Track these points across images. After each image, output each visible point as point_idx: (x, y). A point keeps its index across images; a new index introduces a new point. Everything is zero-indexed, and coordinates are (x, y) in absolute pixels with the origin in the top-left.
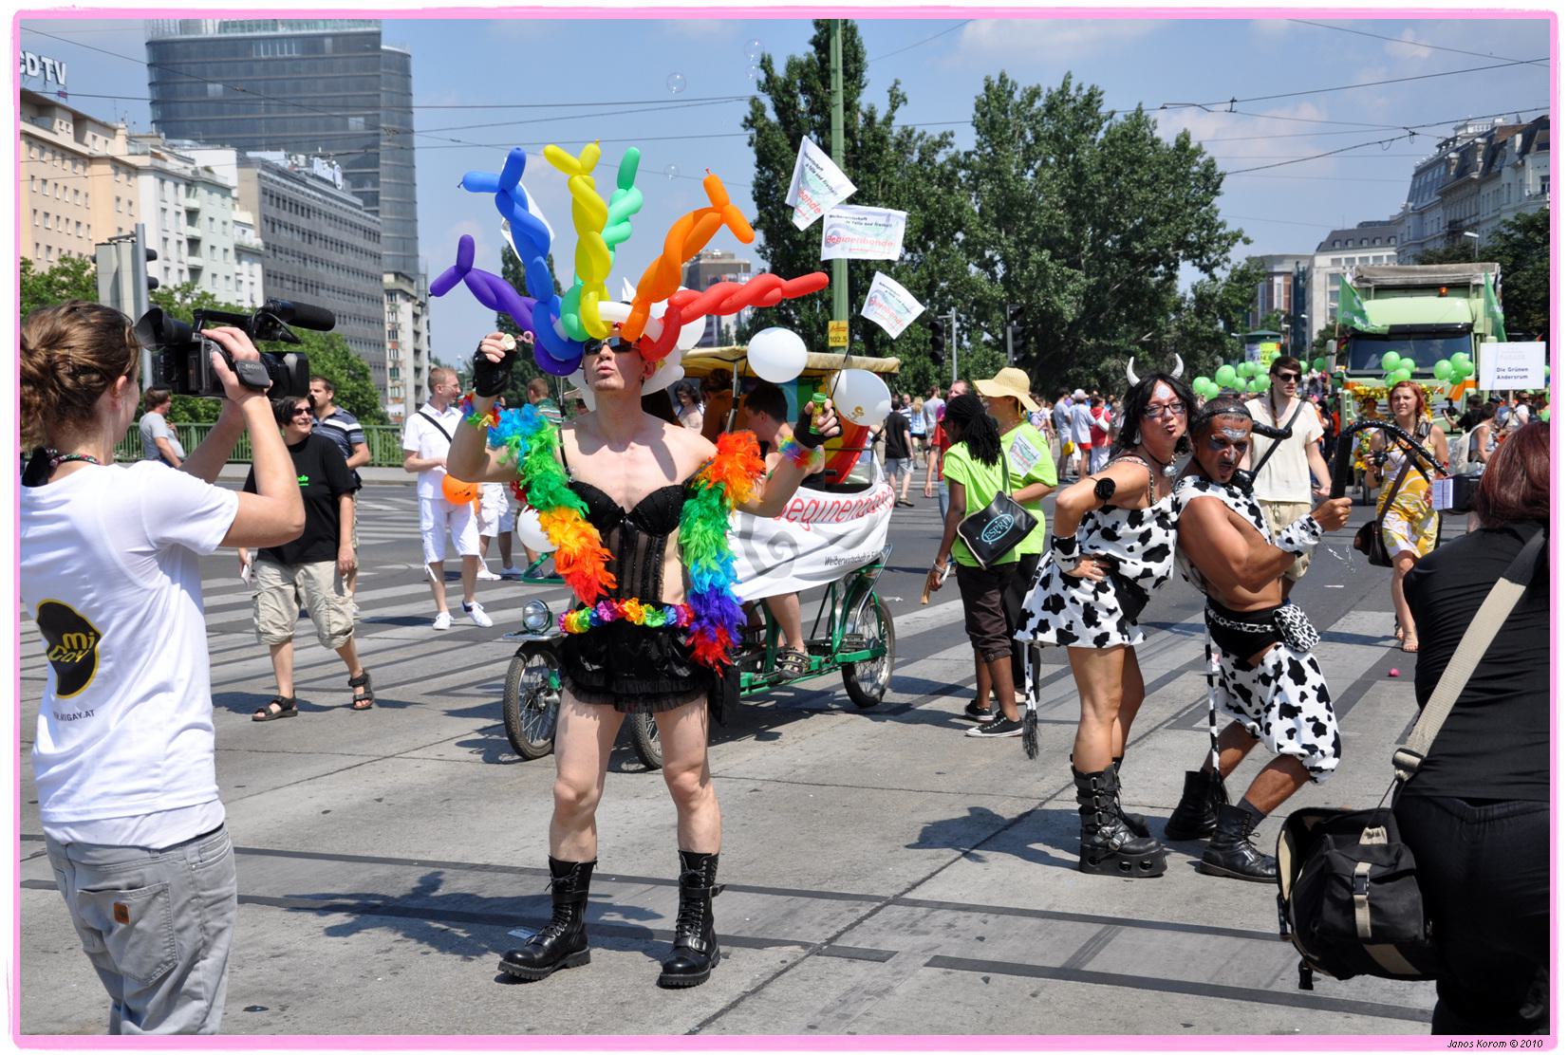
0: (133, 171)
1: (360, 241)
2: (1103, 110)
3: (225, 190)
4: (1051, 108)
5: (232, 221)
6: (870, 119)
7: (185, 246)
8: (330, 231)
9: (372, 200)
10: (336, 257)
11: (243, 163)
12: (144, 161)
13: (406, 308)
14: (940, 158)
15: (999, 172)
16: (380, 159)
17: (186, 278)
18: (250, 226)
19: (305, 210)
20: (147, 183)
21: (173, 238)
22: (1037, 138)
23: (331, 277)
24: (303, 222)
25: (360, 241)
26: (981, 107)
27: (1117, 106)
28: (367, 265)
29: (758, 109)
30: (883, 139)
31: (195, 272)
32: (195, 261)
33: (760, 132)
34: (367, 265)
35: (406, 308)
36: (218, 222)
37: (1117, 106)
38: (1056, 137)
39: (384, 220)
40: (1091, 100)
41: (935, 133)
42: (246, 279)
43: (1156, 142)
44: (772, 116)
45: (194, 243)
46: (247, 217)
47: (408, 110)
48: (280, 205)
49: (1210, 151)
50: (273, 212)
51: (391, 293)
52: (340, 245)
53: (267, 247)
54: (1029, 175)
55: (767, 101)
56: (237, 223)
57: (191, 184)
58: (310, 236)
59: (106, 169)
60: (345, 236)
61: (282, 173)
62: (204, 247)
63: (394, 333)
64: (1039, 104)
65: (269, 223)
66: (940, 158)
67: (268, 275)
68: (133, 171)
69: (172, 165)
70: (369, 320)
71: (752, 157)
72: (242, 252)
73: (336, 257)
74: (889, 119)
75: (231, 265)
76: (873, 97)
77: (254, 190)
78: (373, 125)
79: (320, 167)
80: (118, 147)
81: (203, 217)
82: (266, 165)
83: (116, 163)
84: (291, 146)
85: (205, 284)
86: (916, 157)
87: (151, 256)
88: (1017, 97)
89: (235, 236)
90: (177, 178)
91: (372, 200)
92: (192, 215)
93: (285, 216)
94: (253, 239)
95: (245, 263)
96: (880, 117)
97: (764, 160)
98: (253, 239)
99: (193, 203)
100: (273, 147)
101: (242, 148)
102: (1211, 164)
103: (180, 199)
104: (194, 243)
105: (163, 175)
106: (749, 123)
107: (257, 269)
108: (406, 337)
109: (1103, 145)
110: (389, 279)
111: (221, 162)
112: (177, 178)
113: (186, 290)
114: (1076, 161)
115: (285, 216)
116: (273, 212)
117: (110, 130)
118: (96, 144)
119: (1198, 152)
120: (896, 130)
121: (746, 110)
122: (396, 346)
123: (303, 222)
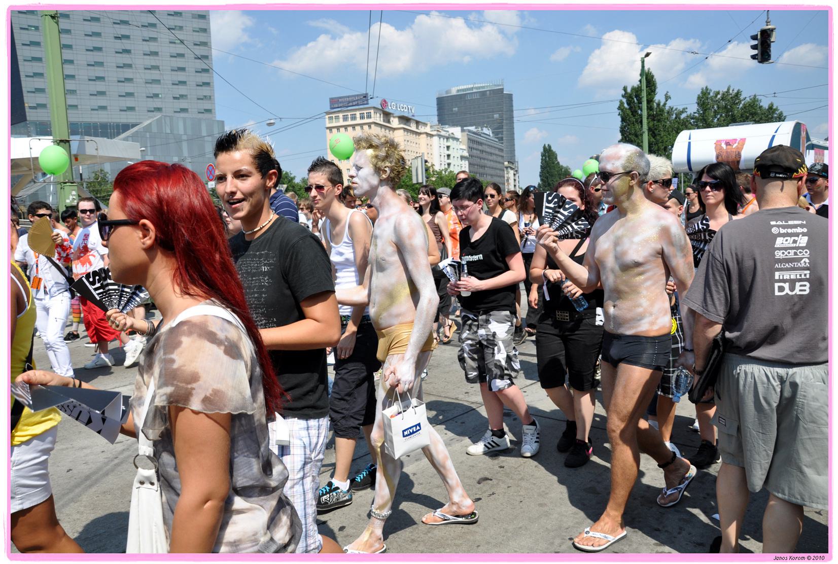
0: (432, 136)
1: (497, 152)
2: (742, 98)
3: (457, 139)
4: (723, 99)
5: (460, 148)
6: (658, 104)
8: (488, 150)
9: (501, 139)
10: (490, 157)
11: (463, 131)
12: (435, 133)
13: (512, 172)
14: (683, 116)
15: (705, 120)
16: (504, 127)
19: (481, 144)
20: (436, 139)
22: (718, 108)
23: (489, 164)
24: (480, 148)
25: (497, 152)
26: (699, 98)
27: (746, 96)
28: (499, 159)
29: (622, 103)
30: (662, 111)
31: (449, 164)
32: (449, 161)
33: (622, 110)
34: (499, 159)
35: (512, 172)
37: (746, 96)
38: (726, 107)
39: (503, 146)
40: (738, 94)
41: (680, 108)
43: (761, 107)
44: (626, 105)
45: (449, 156)
46: (464, 147)
47: (512, 111)
48: (473, 143)
49: (781, 109)
50: (471, 145)
51: (507, 168)
52: (491, 154)
54: (716, 120)
55: (624, 100)
57: (448, 138)
58: (482, 151)
59: (425, 136)
60: (493, 151)
61: (474, 133)
63: (508, 180)
64: (719, 96)
65: (470, 148)
66: (683, 116)
67: (470, 164)
68: (432, 136)
69: (443, 133)
70: (500, 176)
71: (620, 119)
72: (462, 158)
73: (490, 157)
74: (665, 104)
75: (459, 162)
76: (659, 97)
77: (465, 139)
78: (501, 116)
79: (485, 131)
80: (428, 129)
82: (469, 131)
83: (427, 134)
84: (477, 125)
85: (452, 168)
86: (674, 116)
87: (426, 161)
88: (711, 94)
89: (461, 153)
90: (444, 137)
91: (501, 139)
92: (448, 147)
93: (475, 146)
94: (466, 154)
96: (662, 104)
97: (623, 120)
98: (466, 154)
99: (448, 144)
100: (471, 125)
101: (462, 124)
102: (781, 113)
103: (445, 143)
104: (449, 156)
105: (440, 136)
106: (619, 108)
108: (511, 181)
109: (742, 109)
110: (506, 163)
111: (456, 131)
112: (444, 137)
113: (446, 170)
114: (732, 115)
115: (475, 146)
116: (471, 145)
117: (425, 124)
118: (422, 129)
119: (776, 109)
120: (667, 108)
121: (618, 104)
122: (508, 184)
123: (480, 148)
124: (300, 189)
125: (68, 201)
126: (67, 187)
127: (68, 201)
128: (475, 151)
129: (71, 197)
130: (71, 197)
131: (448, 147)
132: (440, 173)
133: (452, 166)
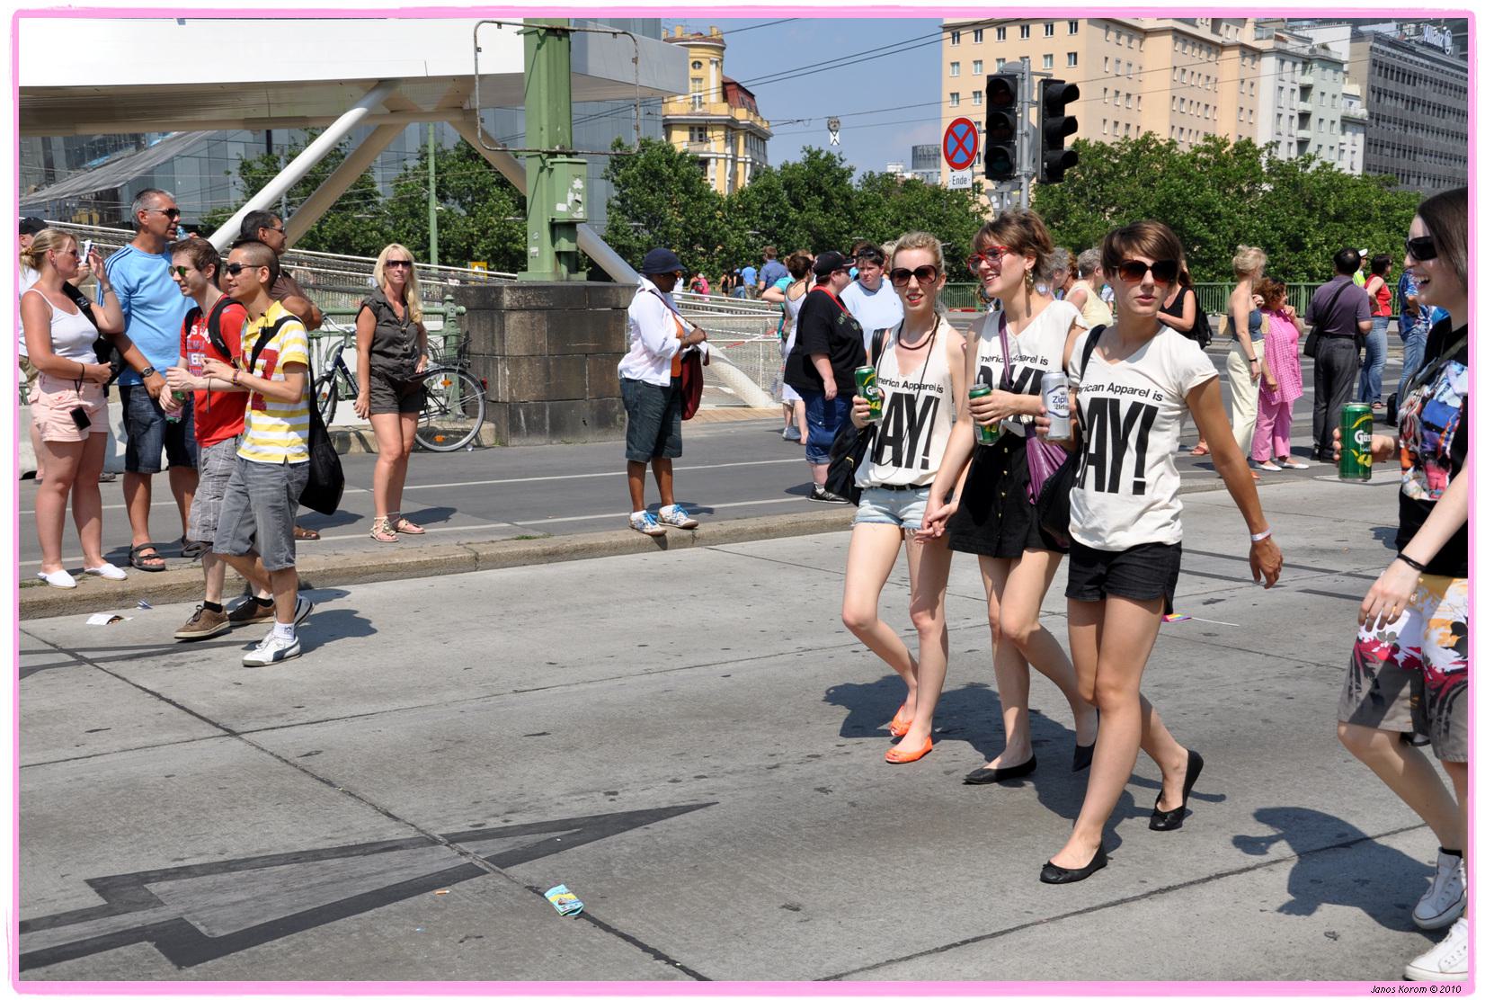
7: (1296, 121)
17: (1295, 148)
18: (1357, 97)
21: (1286, 113)
31: (1303, 144)
32: (1303, 134)
36: (1328, 96)
42: (1348, 148)
53: (1371, 116)
56: (1345, 95)
62: (1313, 120)
65: (1376, 93)
67: (1369, 143)
72: (1348, 123)
81: (1315, 92)
89: (1342, 108)
92: (1306, 91)
94: (1359, 111)
95: (1349, 134)
98: (1359, 111)
104: (1304, 117)
107: (1360, 138)
124: (864, 206)
125: (561, 207)
126: (562, 167)
127: (561, 207)
128: (1389, 103)
129: (571, 197)
130: (571, 197)
131: (1306, 91)
132: (1282, 172)
133: (1311, 149)
